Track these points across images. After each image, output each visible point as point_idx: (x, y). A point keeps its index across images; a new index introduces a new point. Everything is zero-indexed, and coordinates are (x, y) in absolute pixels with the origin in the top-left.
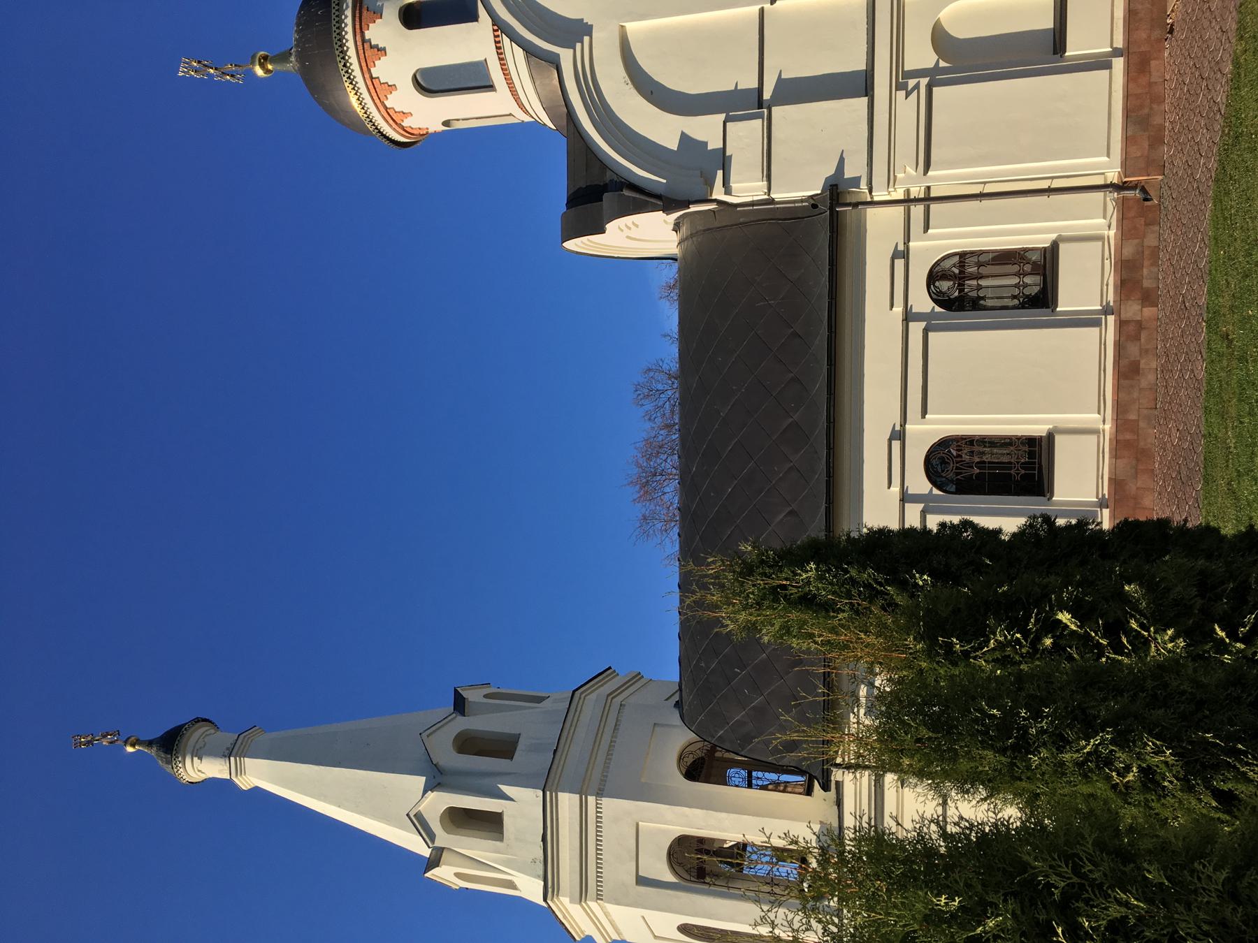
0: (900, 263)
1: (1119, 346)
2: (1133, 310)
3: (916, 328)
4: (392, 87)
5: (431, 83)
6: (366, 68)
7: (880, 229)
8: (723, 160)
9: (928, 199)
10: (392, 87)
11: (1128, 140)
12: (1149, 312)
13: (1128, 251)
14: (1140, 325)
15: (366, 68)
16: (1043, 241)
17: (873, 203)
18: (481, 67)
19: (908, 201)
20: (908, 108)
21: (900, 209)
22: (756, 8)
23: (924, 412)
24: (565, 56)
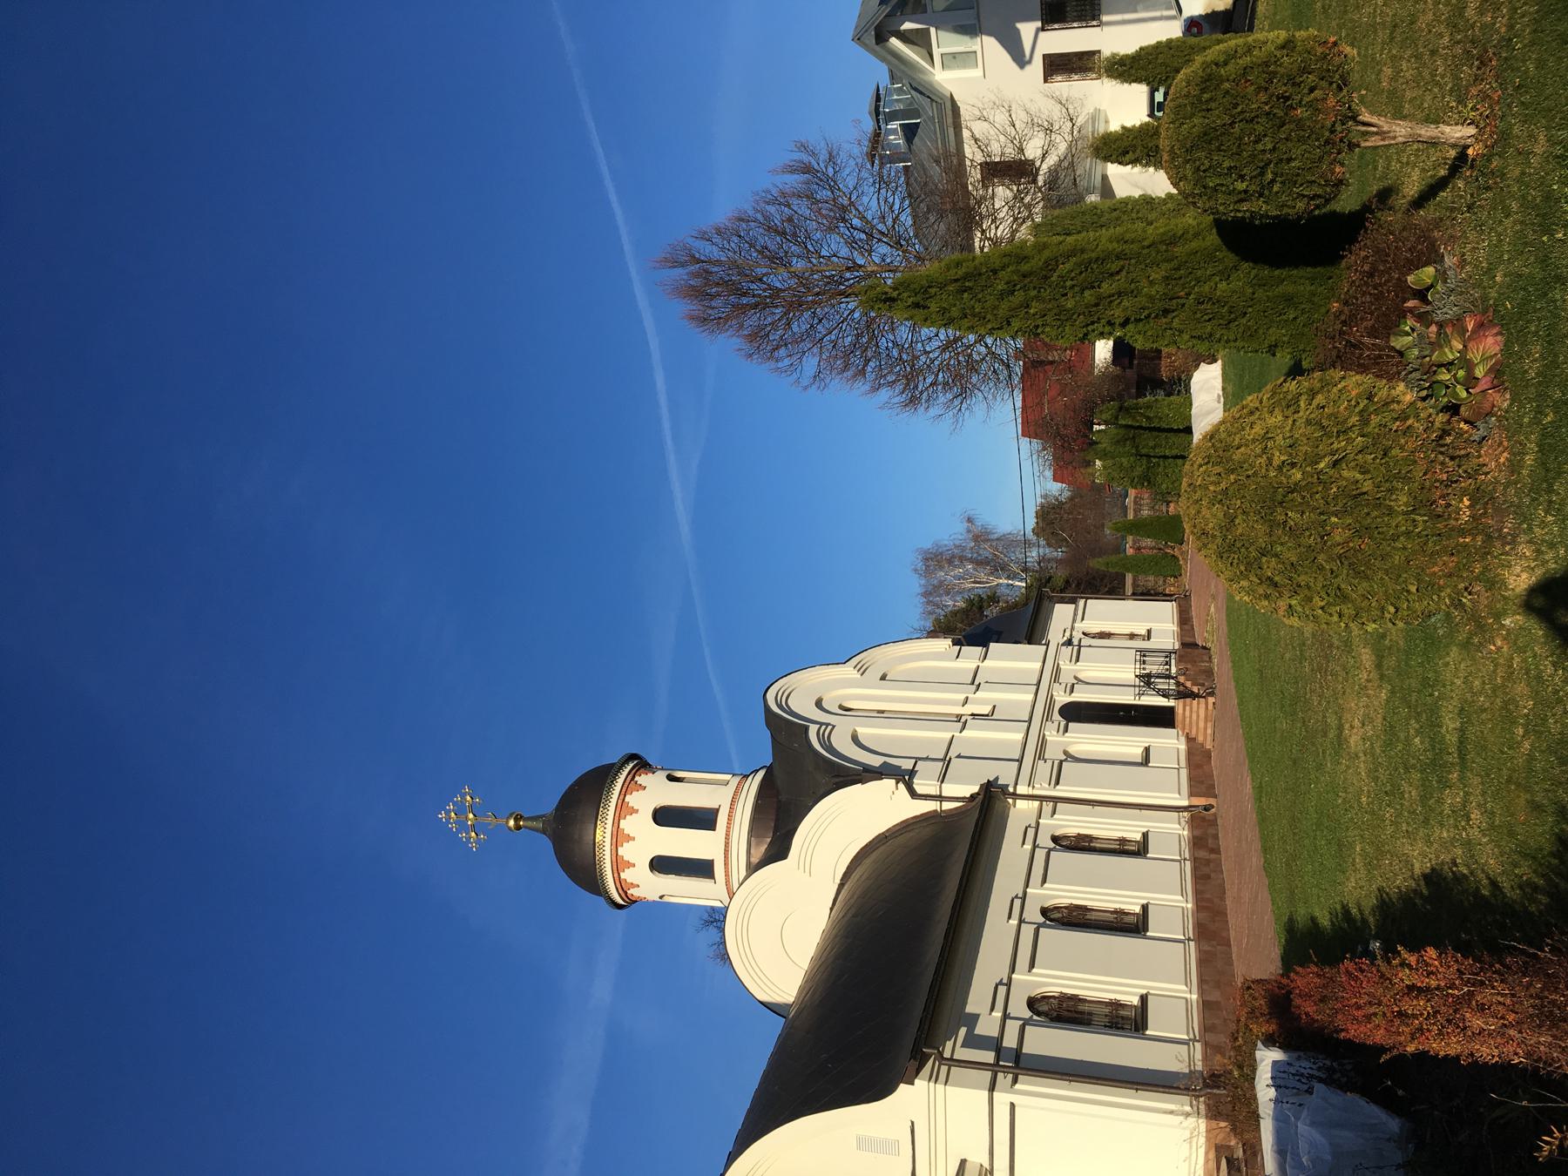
0: (1031, 832)
1: (1195, 869)
2: (1202, 854)
3: (1040, 855)
4: (634, 811)
5: (666, 817)
6: (625, 792)
7: (1022, 810)
8: (912, 773)
9: (1056, 800)
10: (634, 811)
11: (1191, 786)
12: (1213, 856)
13: (1197, 833)
14: (1208, 862)
15: (625, 792)
16: (1138, 837)
17: (1015, 796)
18: (717, 810)
19: (1041, 798)
20: (1044, 769)
21: (1036, 804)
22: (949, 735)
23: (1044, 881)
24: (813, 729)
